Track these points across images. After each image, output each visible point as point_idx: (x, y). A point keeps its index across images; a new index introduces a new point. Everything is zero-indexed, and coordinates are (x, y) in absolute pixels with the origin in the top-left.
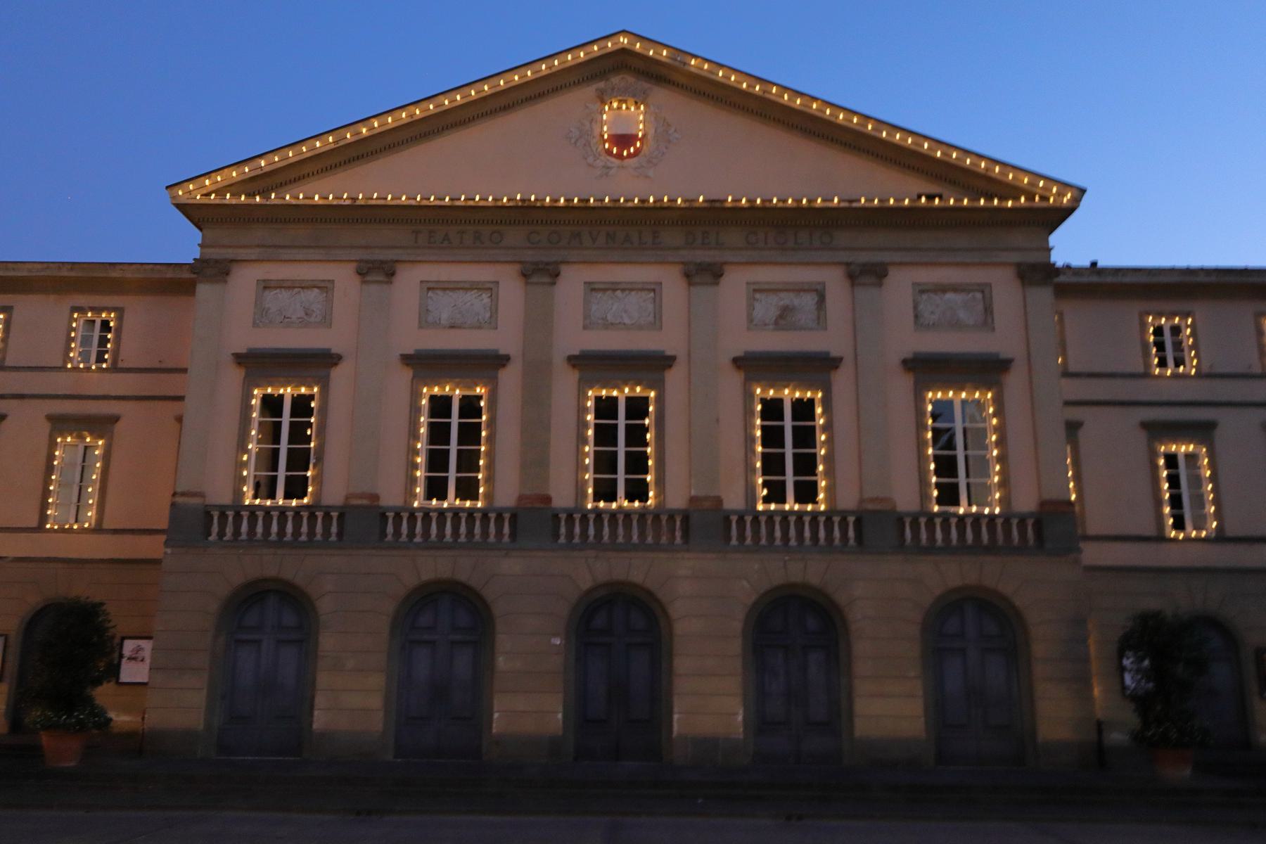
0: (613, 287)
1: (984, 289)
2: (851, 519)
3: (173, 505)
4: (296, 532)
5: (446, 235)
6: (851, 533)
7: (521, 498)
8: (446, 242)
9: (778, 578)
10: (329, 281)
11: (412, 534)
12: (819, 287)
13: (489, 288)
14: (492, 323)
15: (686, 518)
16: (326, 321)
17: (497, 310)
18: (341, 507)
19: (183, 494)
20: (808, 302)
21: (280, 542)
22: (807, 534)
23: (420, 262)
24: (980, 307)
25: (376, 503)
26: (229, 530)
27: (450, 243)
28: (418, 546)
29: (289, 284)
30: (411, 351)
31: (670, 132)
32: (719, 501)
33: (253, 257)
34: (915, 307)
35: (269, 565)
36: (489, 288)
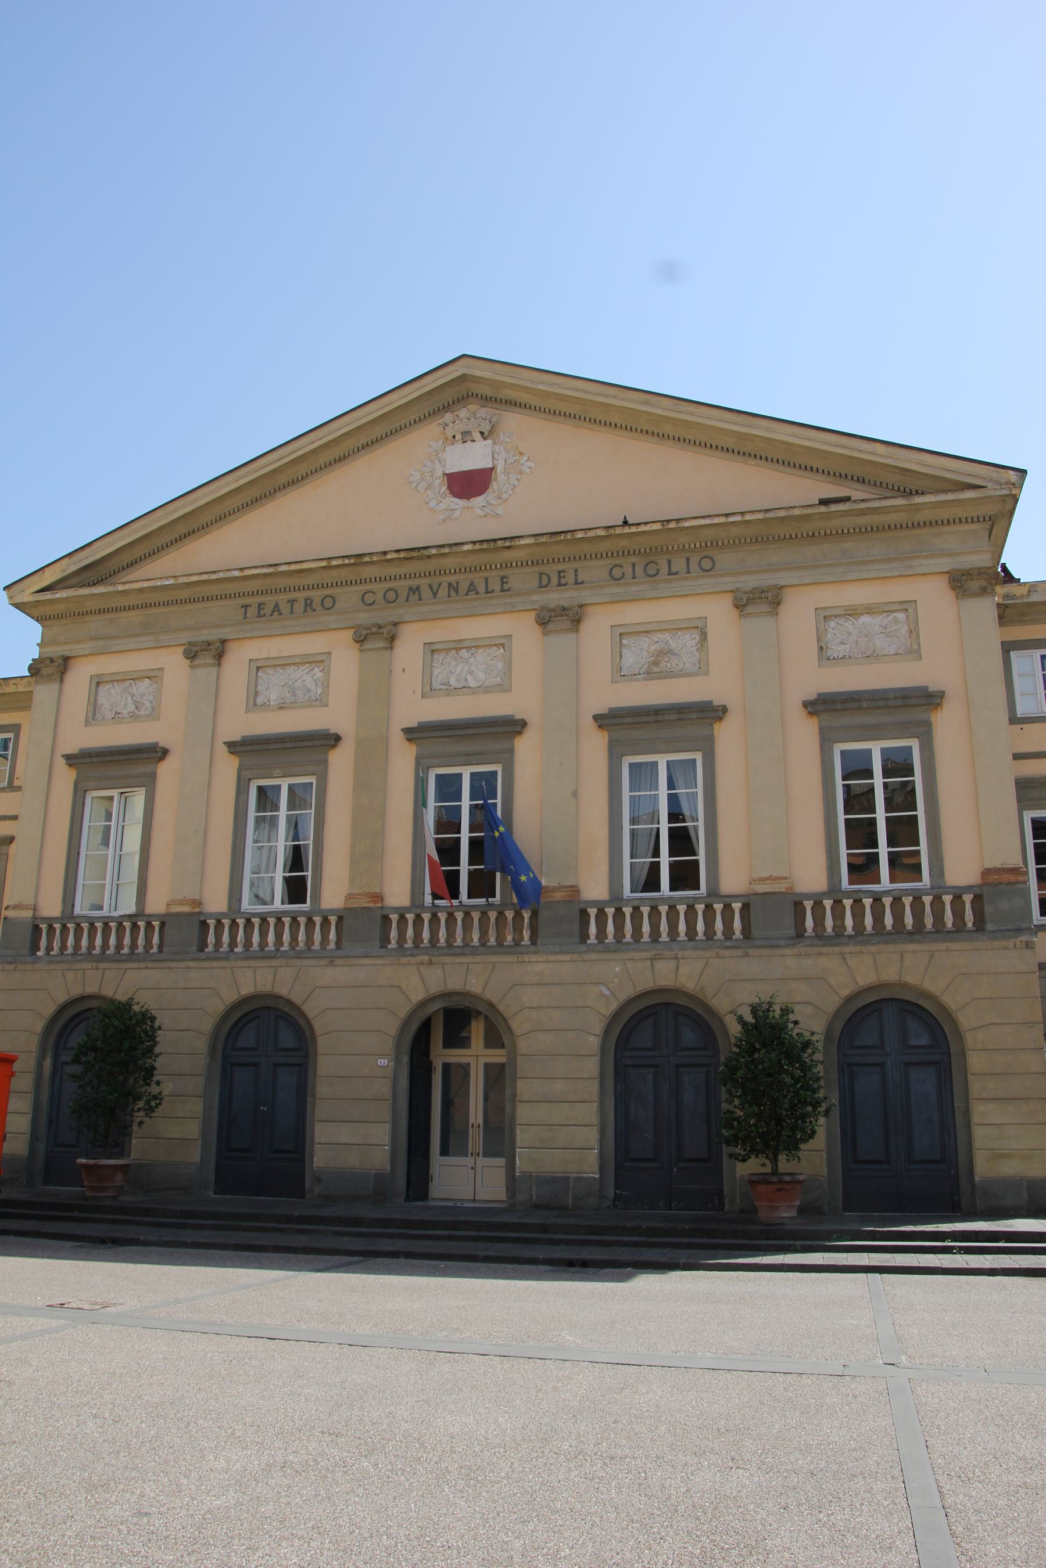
0: (457, 646)
1: (907, 606)
2: (737, 906)
5: (277, 605)
6: (737, 924)
7: (350, 896)
8: (276, 614)
10: (159, 669)
11: (233, 943)
12: (699, 624)
13: (320, 661)
16: (154, 715)
17: (328, 683)
18: (163, 915)
19: (15, 907)
20: (688, 641)
21: (103, 957)
22: (682, 927)
23: (251, 638)
25: (197, 910)
26: (56, 944)
27: (280, 614)
28: (239, 957)
30: (237, 738)
31: (522, 462)
32: (575, 890)
33: (87, 652)
36: (320, 661)
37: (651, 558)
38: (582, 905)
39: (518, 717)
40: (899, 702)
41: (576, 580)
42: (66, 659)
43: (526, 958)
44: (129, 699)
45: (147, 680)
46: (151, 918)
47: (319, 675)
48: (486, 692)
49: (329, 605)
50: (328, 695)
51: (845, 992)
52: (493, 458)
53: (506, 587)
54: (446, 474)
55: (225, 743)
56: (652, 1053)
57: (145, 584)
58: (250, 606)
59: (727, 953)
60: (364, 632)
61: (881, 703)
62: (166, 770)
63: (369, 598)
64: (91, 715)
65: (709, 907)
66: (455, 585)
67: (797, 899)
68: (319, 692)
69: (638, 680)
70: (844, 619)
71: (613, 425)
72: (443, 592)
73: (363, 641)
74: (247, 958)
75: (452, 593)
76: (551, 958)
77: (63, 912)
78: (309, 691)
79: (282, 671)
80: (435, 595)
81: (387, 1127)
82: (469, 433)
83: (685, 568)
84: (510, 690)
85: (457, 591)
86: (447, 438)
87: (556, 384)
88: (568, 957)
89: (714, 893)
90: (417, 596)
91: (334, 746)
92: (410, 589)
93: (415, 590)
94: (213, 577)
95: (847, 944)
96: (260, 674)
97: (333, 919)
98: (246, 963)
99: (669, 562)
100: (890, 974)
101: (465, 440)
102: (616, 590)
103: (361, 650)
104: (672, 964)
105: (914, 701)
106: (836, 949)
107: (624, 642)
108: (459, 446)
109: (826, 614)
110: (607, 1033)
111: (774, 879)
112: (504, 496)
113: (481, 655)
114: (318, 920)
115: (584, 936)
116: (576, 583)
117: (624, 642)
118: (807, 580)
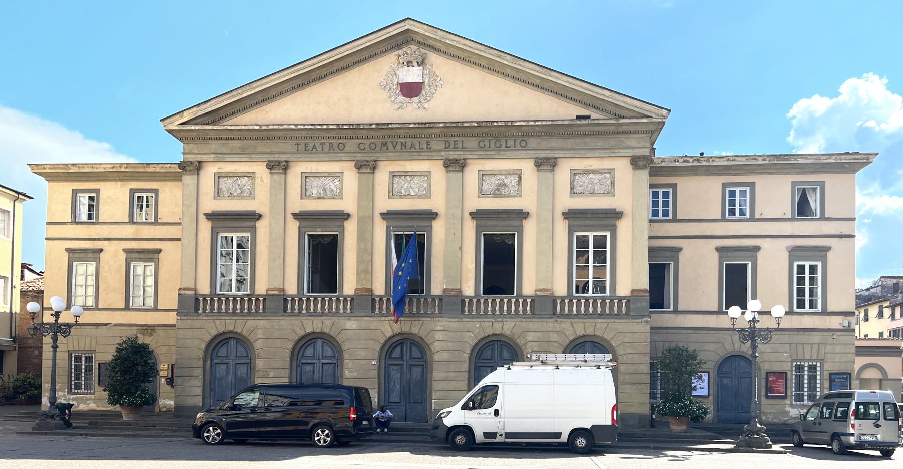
0: (405, 174)
1: (611, 171)
2: (529, 300)
3: (179, 294)
4: (242, 308)
5: (314, 145)
6: (529, 308)
7: (356, 290)
8: (314, 150)
9: (489, 332)
10: (253, 173)
11: (300, 309)
12: (518, 173)
14: (339, 196)
15: (441, 299)
16: (252, 196)
17: (342, 188)
19: (184, 289)
20: (512, 181)
21: (234, 313)
24: (609, 181)
25: (282, 293)
27: (316, 150)
28: (304, 315)
29: (231, 175)
30: (298, 212)
32: (460, 291)
33: (211, 160)
34: (572, 182)
35: (229, 325)
36: (338, 176)
37: (498, 138)
38: (463, 298)
39: (434, 211)
40: (603, 216)
41: (462, 146)
42: (200, 162)
43: (437, 319)
44: (237, 187)
45: (246, 178)
46: (259, 297)
47: (337, 183)
48: (418, 198)
49: (341, 148)
50: (342, 193)
51: (572, 338)
52: (423, 77)
53: (429, 147)
54: (399, 83)
55: (292, 214)
56: (491, 361)
57: (243, 127)
58: (300, 144)
59: (524, 320)
60: (360, 164)
61: (596, 216)
62: (259, 224)
63: (362, 146)
64: (216, 193)
65: (517, 300)
66: (404, 143)
67: (555, 298)
68: (337, 192)
69: (489, 197)
70: (582, 175)
71: (482, 66)
72: (398, 147)
73: (359, 168)
74: (309, 316)
75: (403, 147)
76: (448, 320)
77: (210, 292)
78: (332, 191)
79: (318, 179)
80: (395, 147)
81: (376, 390)
82: (411, 62)
83: (513, 144)
84: (430, 198)
85: (405, 146)
86: (399, 63)
87: (455, 41)
88: (456, 320)
89: (520, 295)
90: (385, 147)
91: (346, 219)
92: (382, 143)
93: (385, 144)
94: (281, 127)
95: (574, 318)
96: (307, 180)
97: (349, 299)
98: (309, 318)
99: (506, 141)
100: (590, 331)
101: (409, 65)
102: (481, 153)
103: (358, 173)
104: (501, 324)
105: (609, 216)
106: (569, 320)
107: (484, 178)
108: (406, 68)
109: (575, 172)
110: (472, 352)
111: (544, 290)
112: (428, 98)
113: (416, 179)
114: (341, 299)
115: (463, 311)
116: (462, 148)
117: (484, 178)
118: (568, 156)
